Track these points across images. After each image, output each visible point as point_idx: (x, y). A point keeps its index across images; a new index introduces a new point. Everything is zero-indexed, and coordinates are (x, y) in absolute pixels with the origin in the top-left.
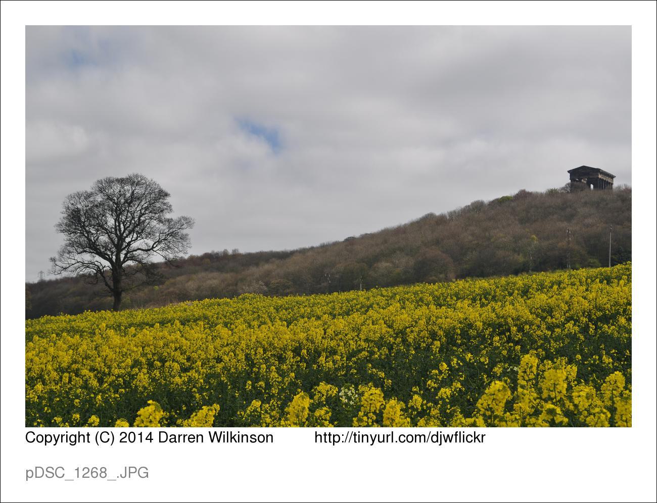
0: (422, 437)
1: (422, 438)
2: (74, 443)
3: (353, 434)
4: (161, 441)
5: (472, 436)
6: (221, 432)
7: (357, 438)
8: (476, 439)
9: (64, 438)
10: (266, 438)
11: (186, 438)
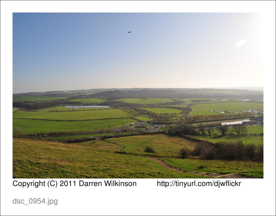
0: (210, 183)
1: (210, 183)
2: (37, 187)
3: (176, 182)
4: (81, 185)
5: (234, 183)
6: (111, 181)
7: (177, 184)
8: (236, 185)
9: (32, 184)
11: (93, 184)
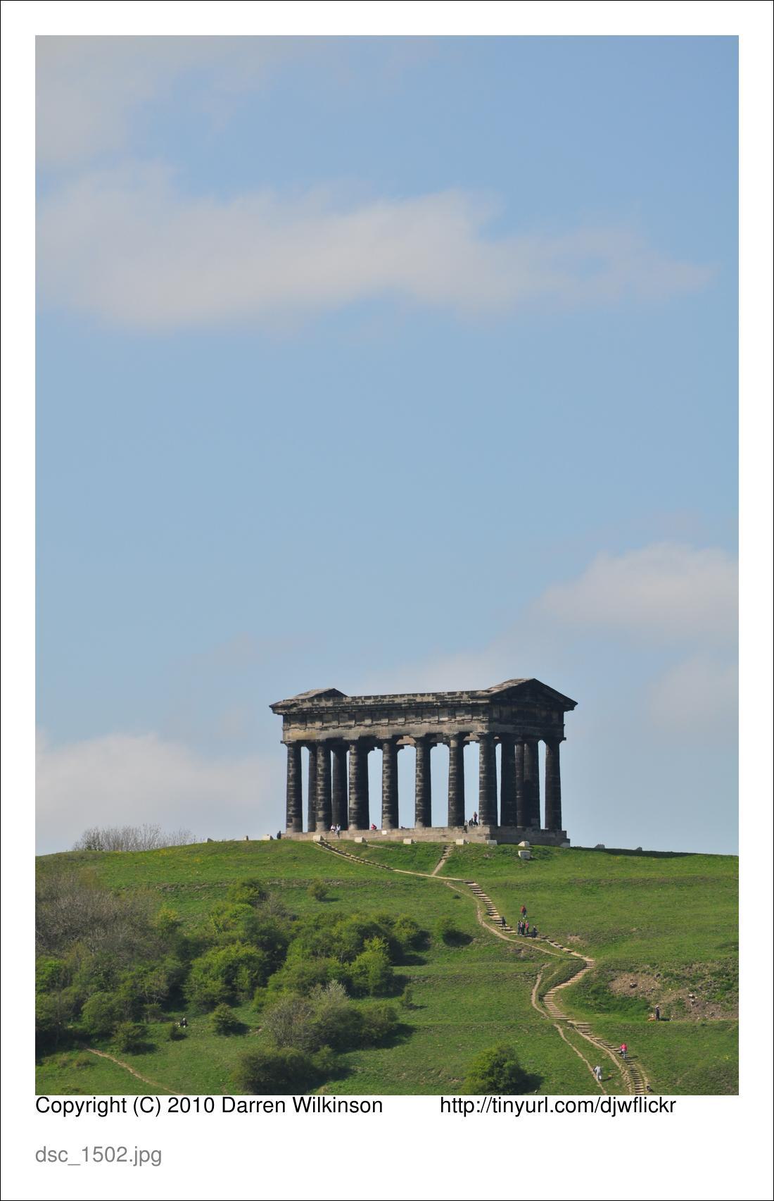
1: (589, 1105)
3: (492, 1100)
4: (226, 1109)
5: (657, 1104)
6: (310, 1098)
8: (663, 1108)
10: (372, 1107)
11: (261, 1106)
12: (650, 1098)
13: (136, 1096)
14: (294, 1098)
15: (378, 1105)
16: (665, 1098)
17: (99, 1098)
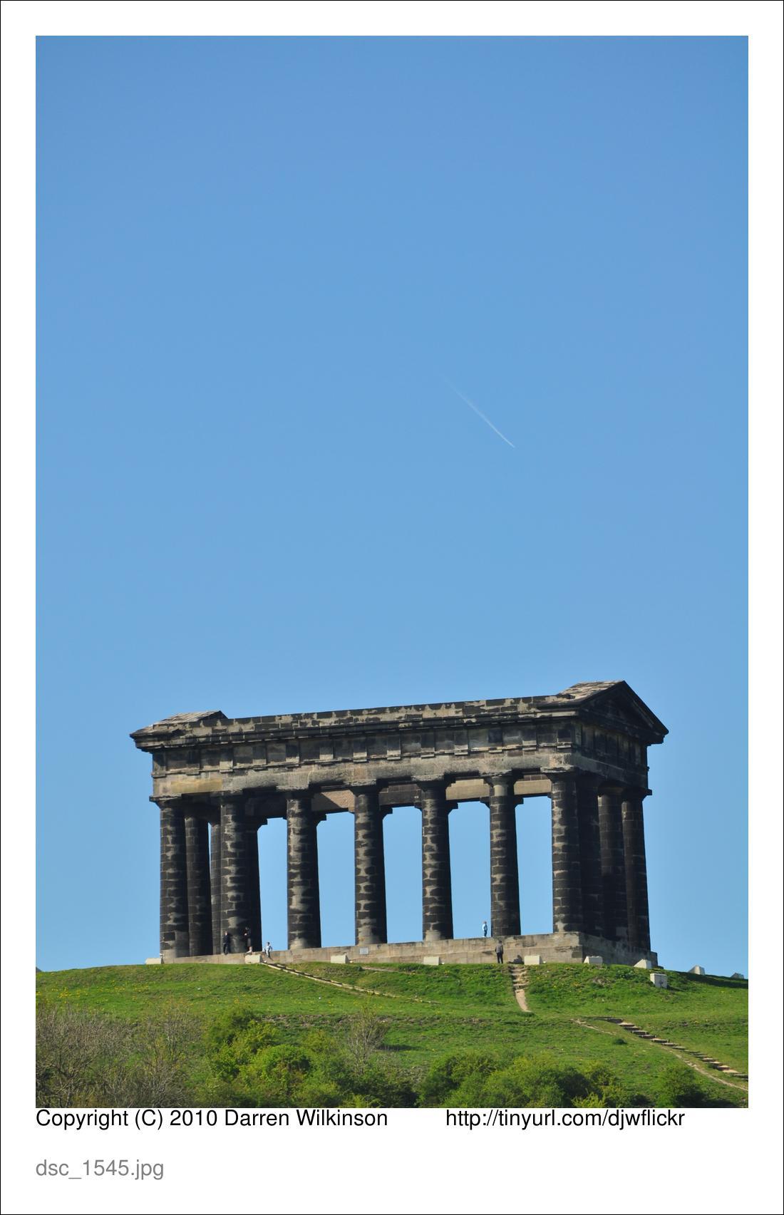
1: (597, 1118)
3: (499, 1113)
4: (229, 1122)
5: (665, 1117)
6: (314, 1111)
8: (672, 1121)
9: (92, 1119)
10: (377, 1120)
11: (264, 1119)
12: (658, 1111)
13: (138, 1109)
14: (298, 1111)
15: (382, 1118)
16: (674, 1111)
17: (100, 1111)
